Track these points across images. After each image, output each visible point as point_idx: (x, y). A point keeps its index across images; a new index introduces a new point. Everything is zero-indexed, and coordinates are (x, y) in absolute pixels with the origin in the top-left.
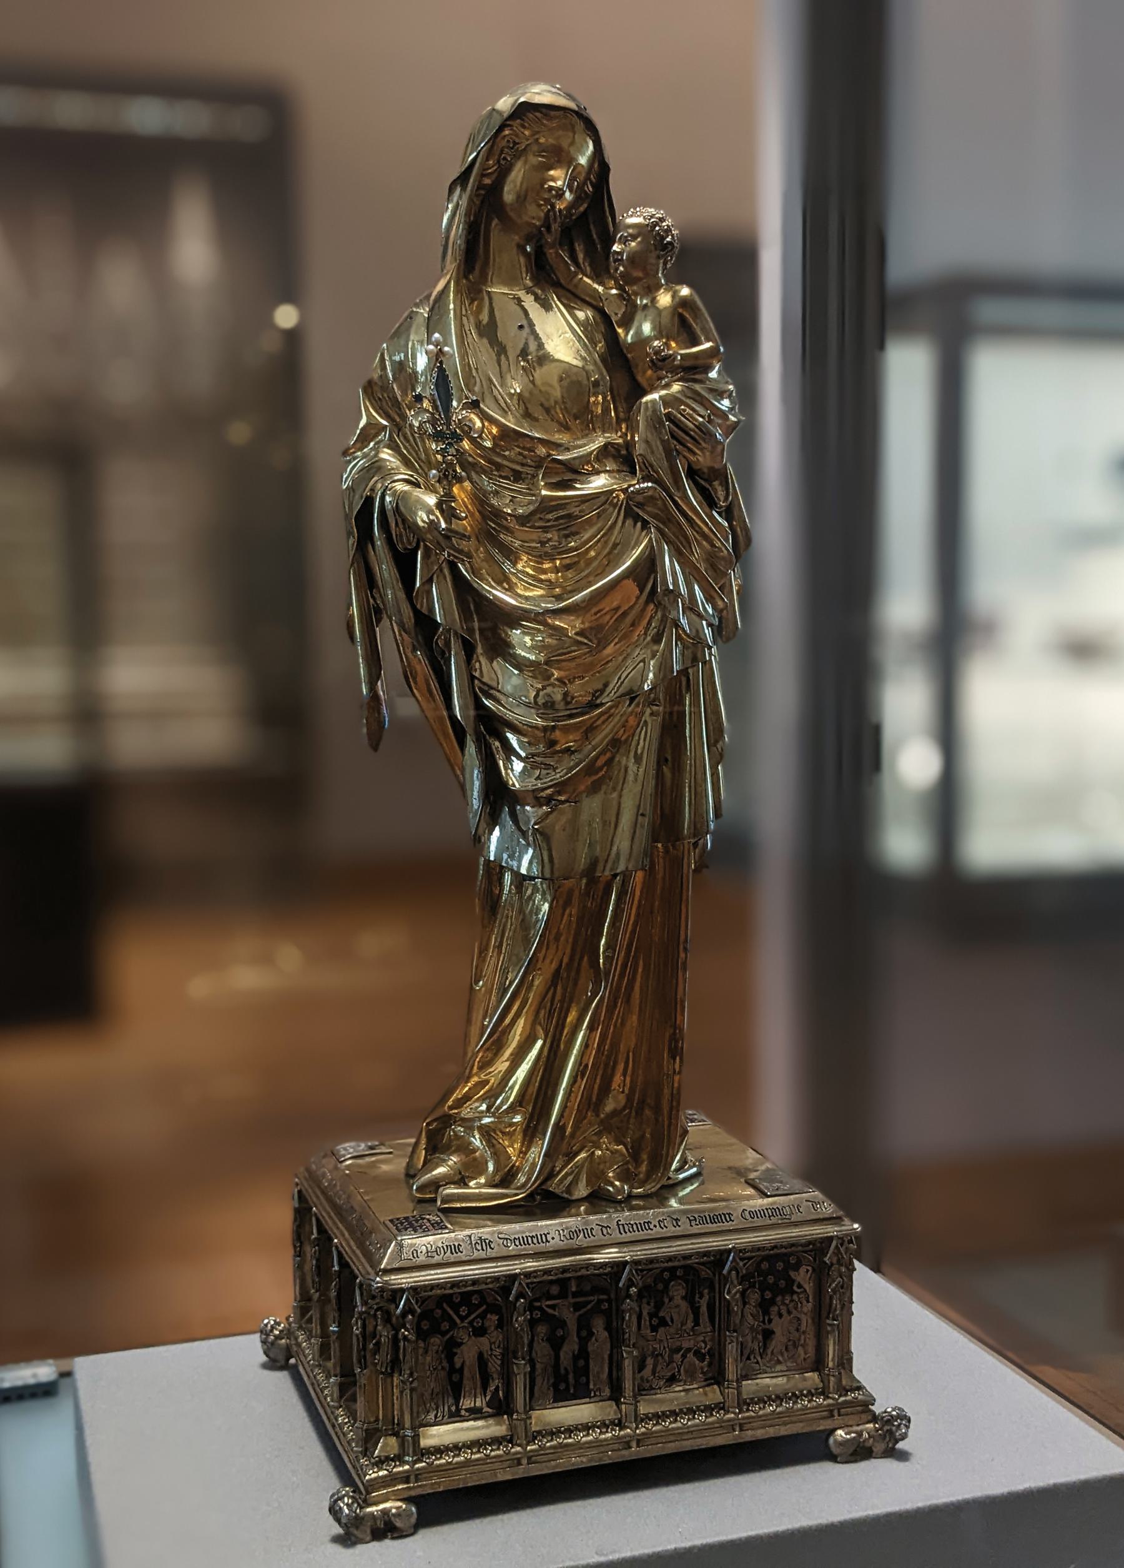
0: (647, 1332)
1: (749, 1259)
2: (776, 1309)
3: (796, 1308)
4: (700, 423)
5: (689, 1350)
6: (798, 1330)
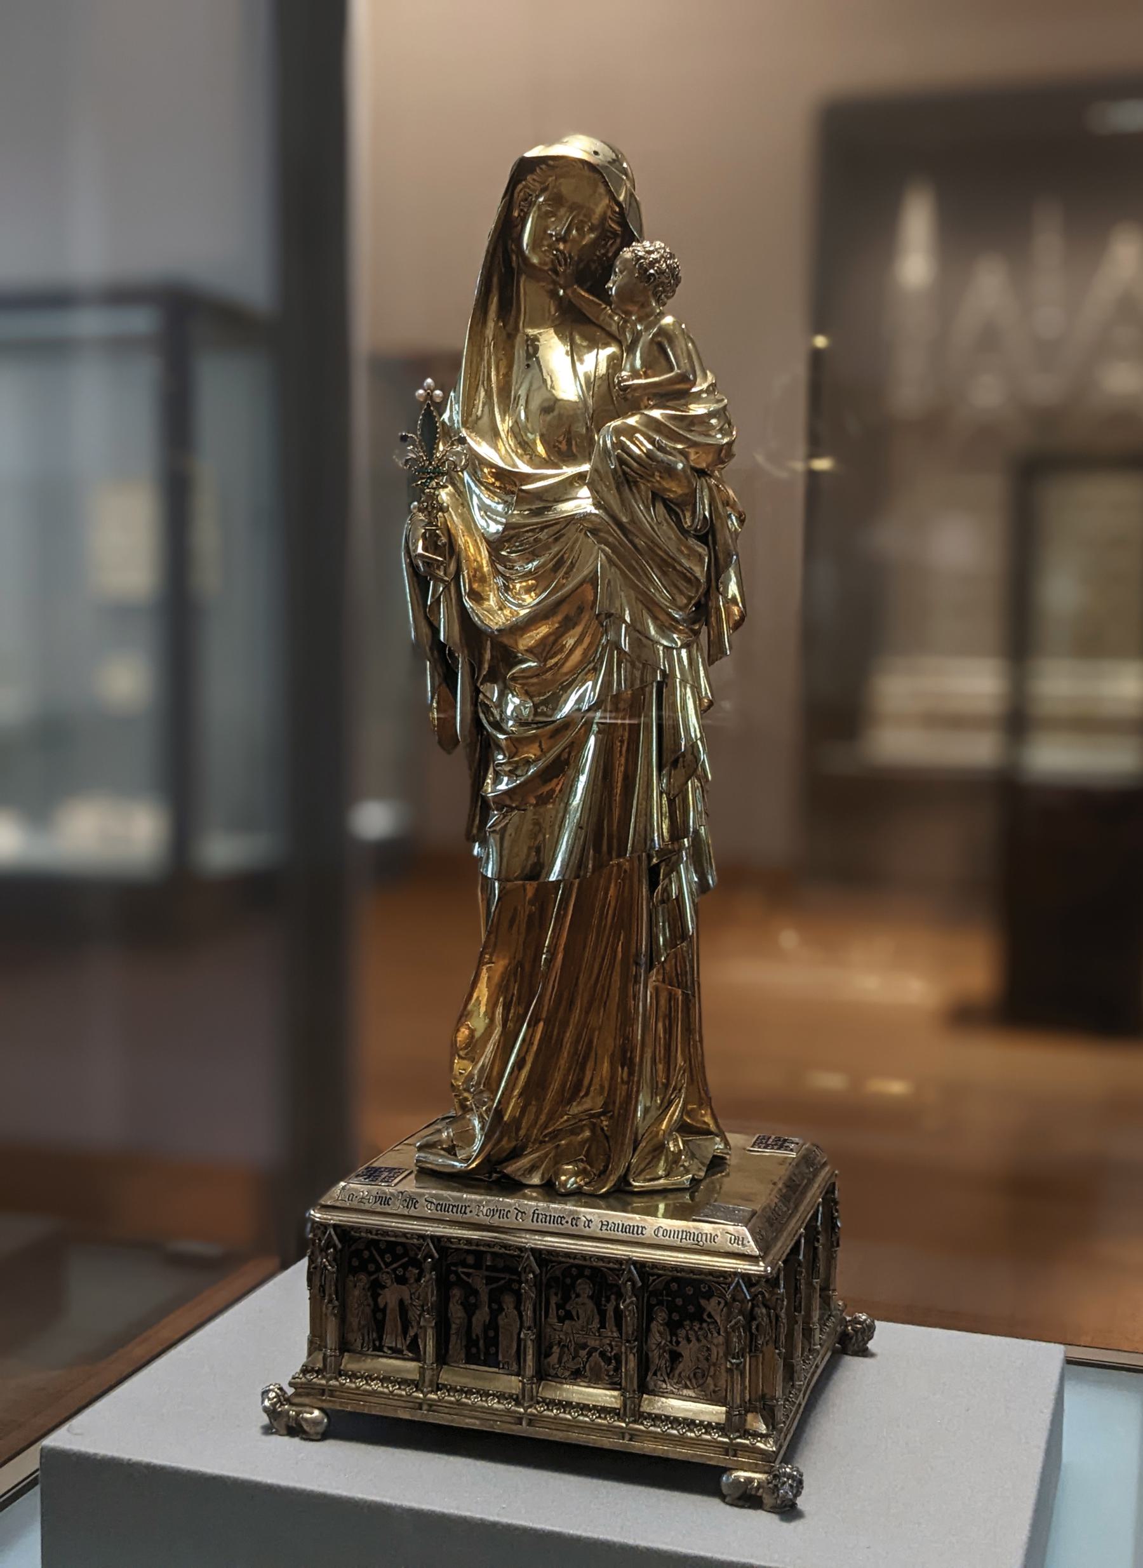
0: (553, 1320)
1: (660, 1276)
2: (684, 1332)
3: (706, 1337)
4: (648, 450)
5: (595, 1349)
6: (707, 1360)
